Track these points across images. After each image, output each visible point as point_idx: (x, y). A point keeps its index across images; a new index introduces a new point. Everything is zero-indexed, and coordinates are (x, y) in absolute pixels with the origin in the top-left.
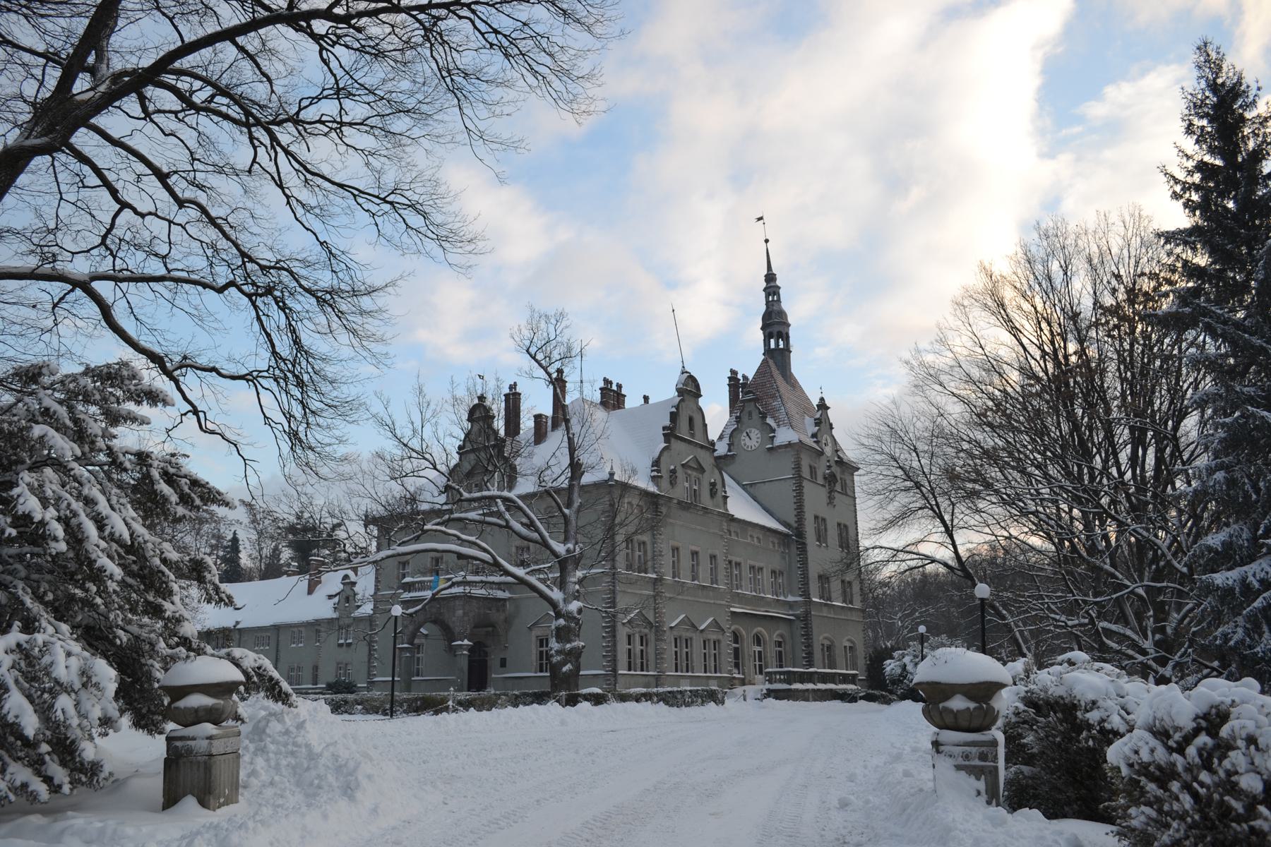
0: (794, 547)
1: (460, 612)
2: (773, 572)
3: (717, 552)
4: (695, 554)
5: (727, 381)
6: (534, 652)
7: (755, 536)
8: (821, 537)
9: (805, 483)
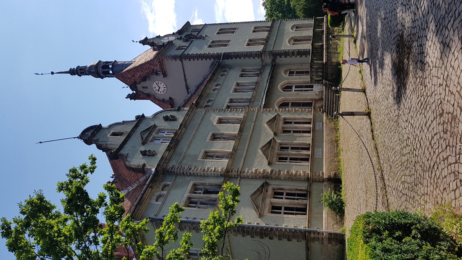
2: (242, 76)
3: (217, 117)
7: (214, 87)
8: (225, 44)
9: (186, 53)
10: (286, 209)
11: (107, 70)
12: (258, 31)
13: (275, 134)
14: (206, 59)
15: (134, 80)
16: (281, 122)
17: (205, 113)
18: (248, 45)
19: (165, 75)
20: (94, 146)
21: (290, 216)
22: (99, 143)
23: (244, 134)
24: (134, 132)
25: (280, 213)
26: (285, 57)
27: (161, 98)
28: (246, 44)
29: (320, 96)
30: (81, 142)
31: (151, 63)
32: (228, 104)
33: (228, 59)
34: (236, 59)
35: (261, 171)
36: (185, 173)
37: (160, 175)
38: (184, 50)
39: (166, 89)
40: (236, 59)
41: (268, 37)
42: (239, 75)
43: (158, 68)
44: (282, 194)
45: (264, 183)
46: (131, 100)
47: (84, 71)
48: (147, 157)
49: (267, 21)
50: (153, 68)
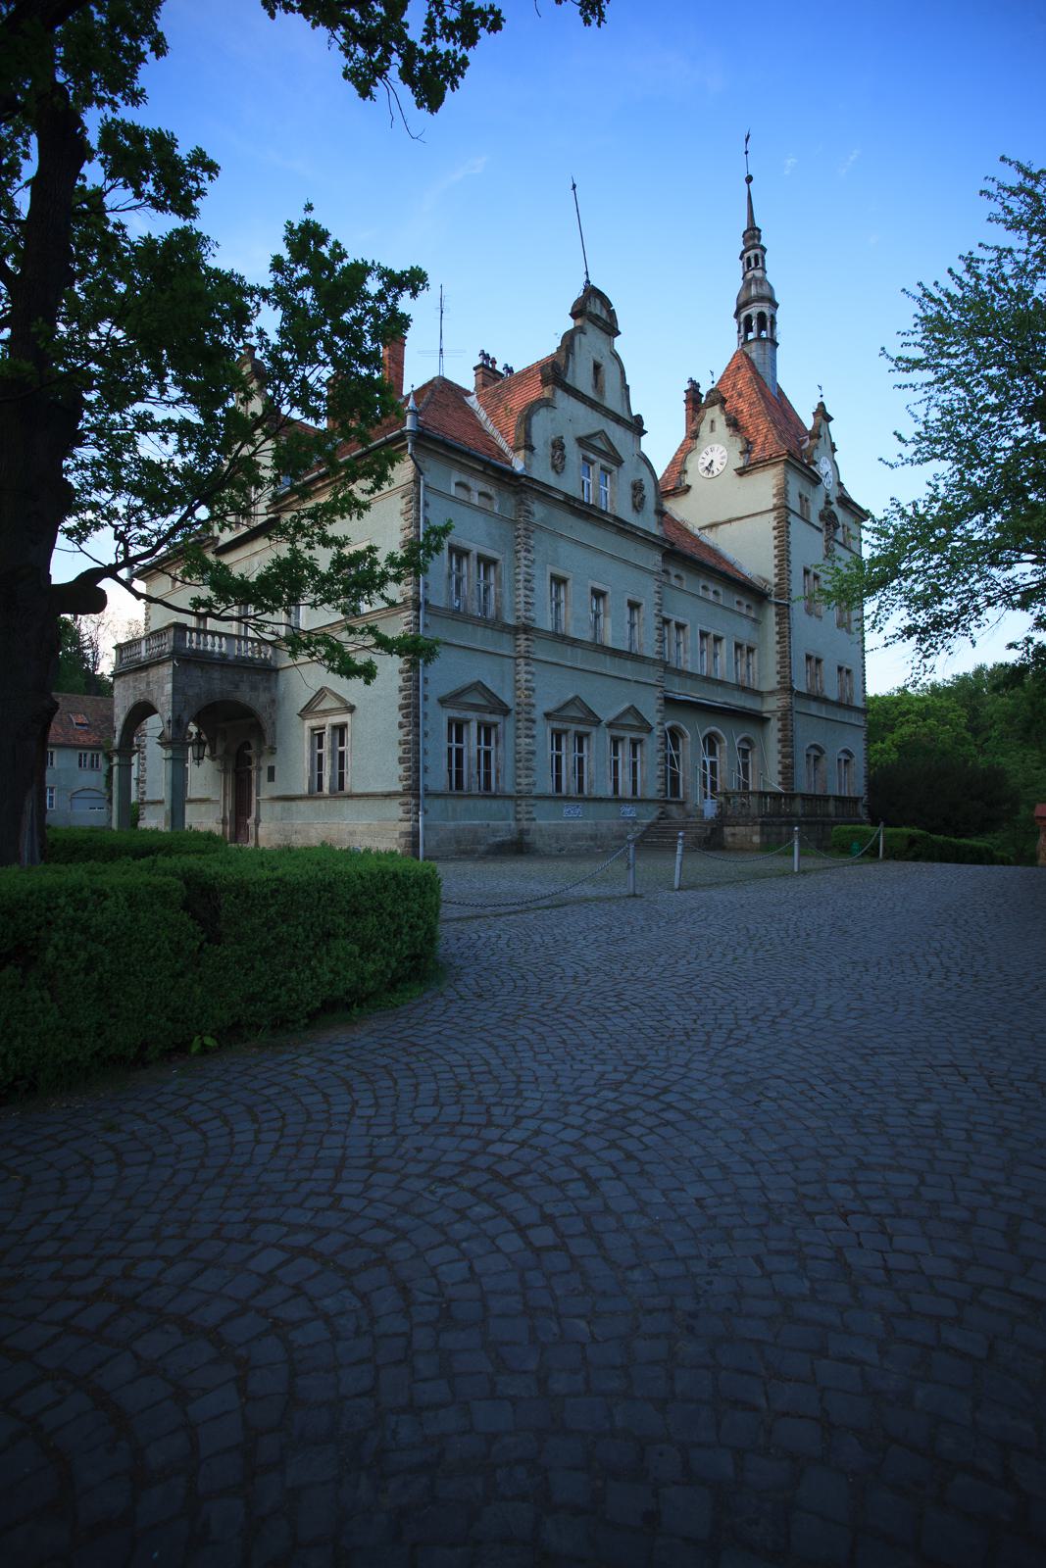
0: (772, 611)
1: (169, 687)
2: (738, 646)
3: (643, 601)
4: (598, 595)
5: (684, 396)
6: (307, 755)
9: (792, 518)
10: (459, 752)
11: (755, 328)
12: (840, 680)
13: (610, 725)
14: (776, 566)
15: (731, 397)
16: (634, 735)
17: (652, 573)
18: (809, 658)
19: (742, 472)
20: (570, 324)
21: (446, 760)
22: (577, 338)
24: (603, 415)
25: (450, 741)
26: (780, 741)
27: (689, 466)
28: (811, 653)
29: (694, 814)
30: (577, 292)
31: (769, 437)
32: (673, 624)
33: (777, 615)
34: (778, 633)
35: (533, 701)
36: (519, 540)
37: (512, 485)
38: (798, 511)
39: (710, 476)
40: (778, 633)
41: (825, 701)
42: (740, 641)
43: (757, 454)
44: (488, 743)
45: (506, 706)
46: (686, 391)
47: (753, 265)
48: (550, 450)
49: (865, 699)
50: (759, 441)
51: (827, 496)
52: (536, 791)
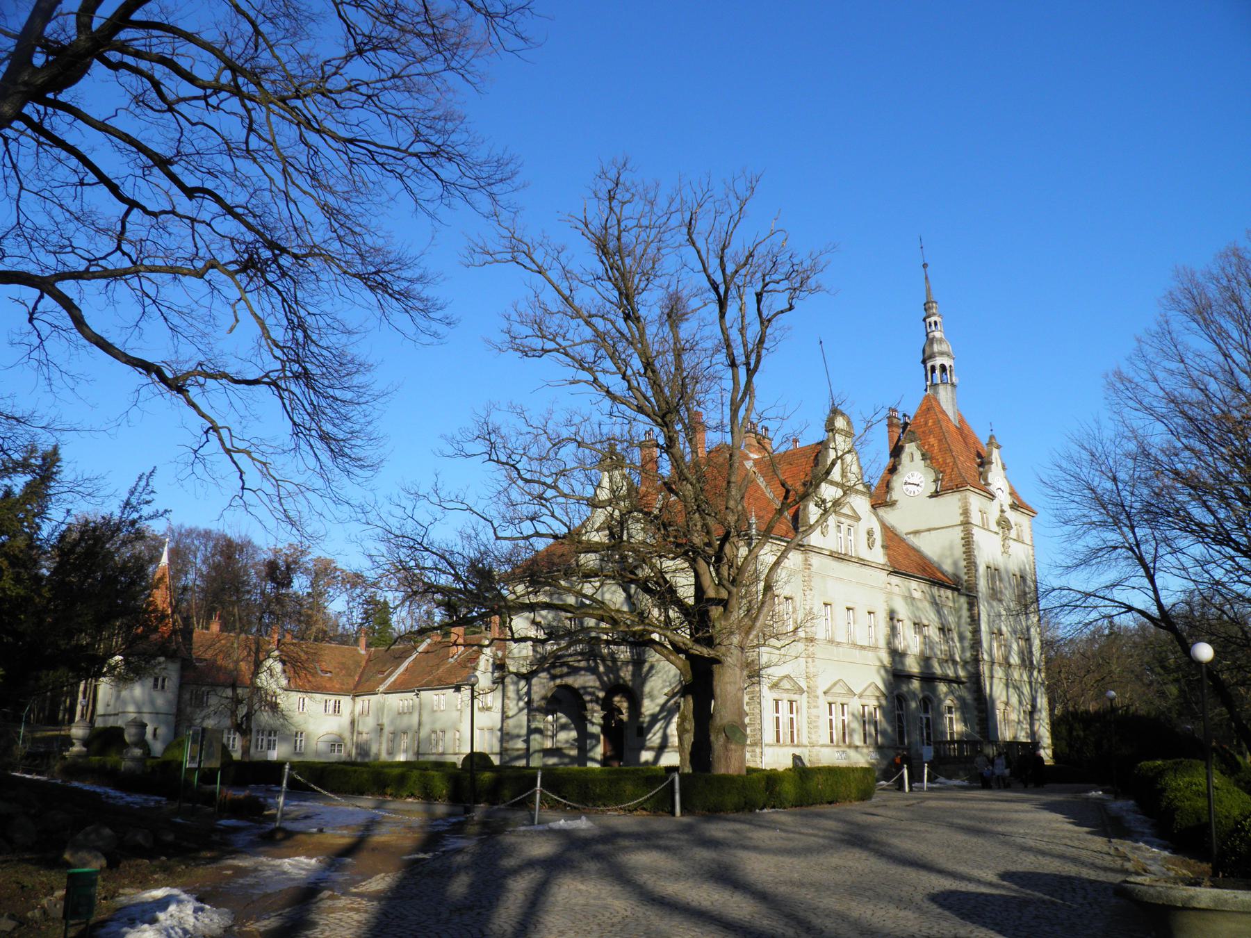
9: (975, 531)
13: (861, 696)
19: (936, 494)
23: (857, 652)
51: (1001, 506)
52: (821, 742)
